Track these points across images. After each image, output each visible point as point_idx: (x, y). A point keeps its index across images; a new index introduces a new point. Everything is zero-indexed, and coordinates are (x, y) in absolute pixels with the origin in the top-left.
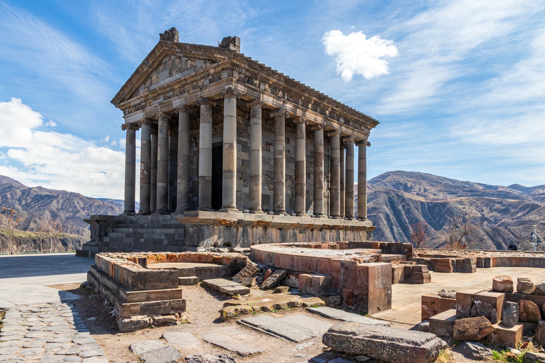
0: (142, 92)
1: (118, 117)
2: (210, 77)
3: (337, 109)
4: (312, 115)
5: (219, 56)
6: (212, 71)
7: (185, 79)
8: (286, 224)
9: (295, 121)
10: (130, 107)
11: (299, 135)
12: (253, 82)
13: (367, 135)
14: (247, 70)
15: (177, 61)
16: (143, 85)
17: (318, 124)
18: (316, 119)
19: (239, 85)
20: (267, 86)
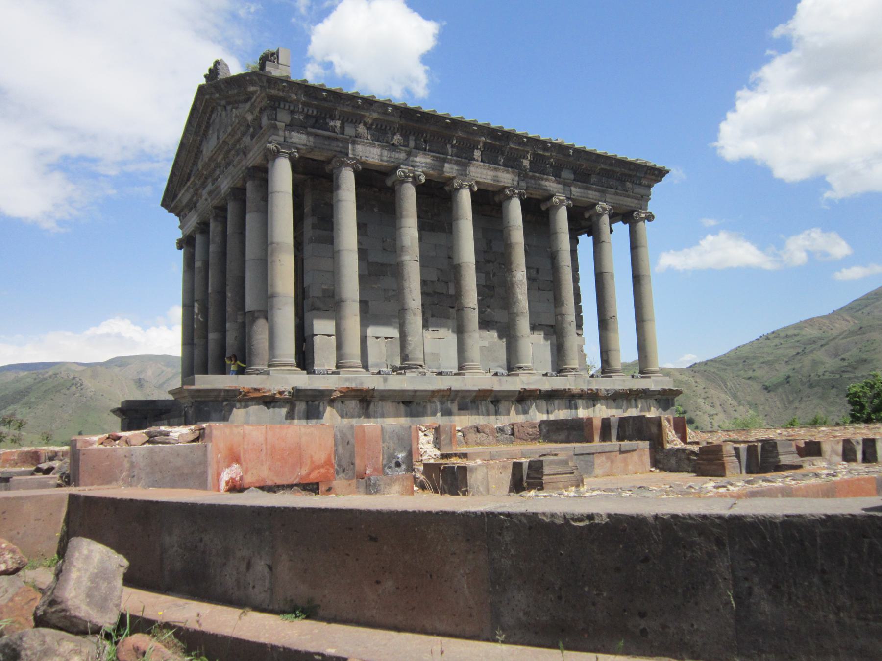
2: (252, 130)
3: (548, 154)
4: (485, 172)
6: (250, 118)
8: (416, 391)
9: (447, 188)
12: (327, 124)
13: (646, 198)
14: (304, 104)
15: (224, 113)
17: (505, 187)
19: (294, 134)
20: (361, 129)
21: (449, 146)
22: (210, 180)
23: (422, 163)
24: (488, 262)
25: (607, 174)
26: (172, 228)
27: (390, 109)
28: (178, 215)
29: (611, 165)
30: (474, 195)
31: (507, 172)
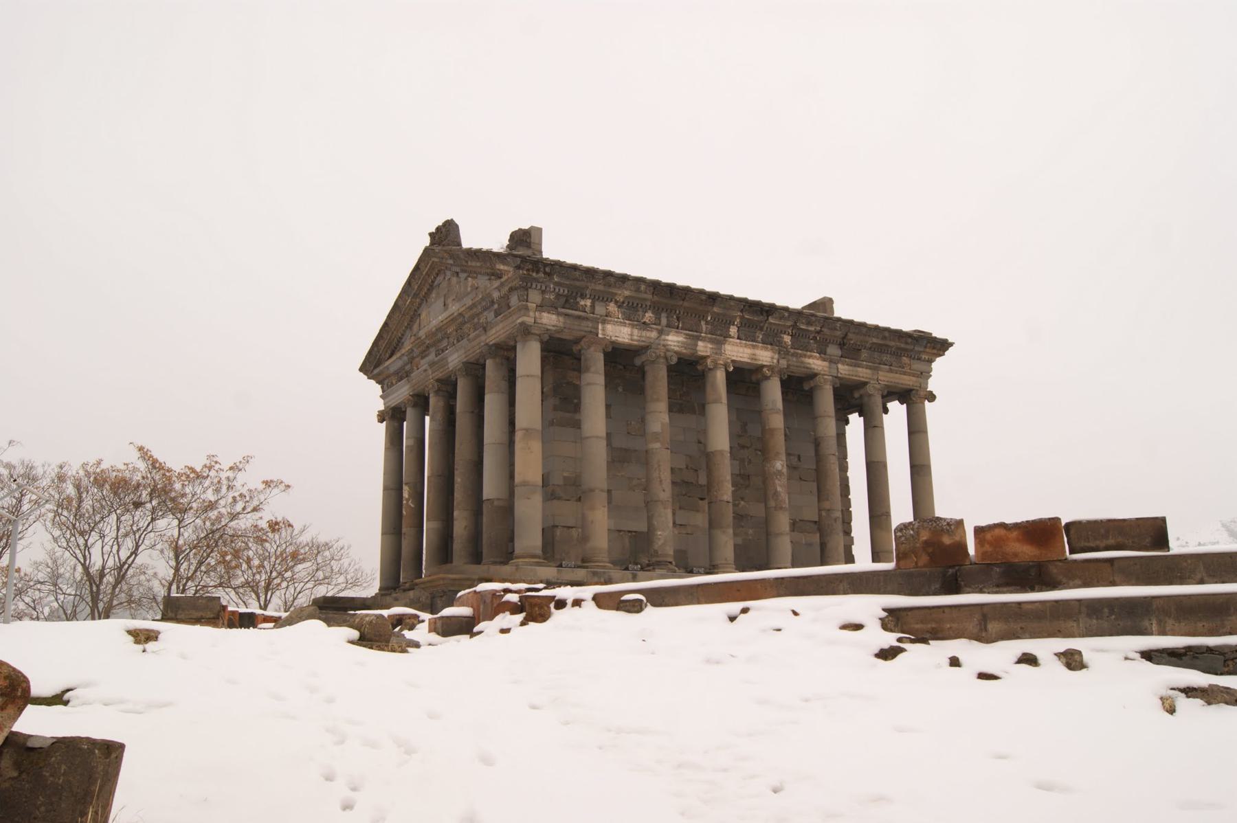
0: (407, 346)
1: (371, 396)
2: (496, 306)
3: (812, 329)
4: (741, 350)
5: (502, 267)
6: (496, 295)
7: (460, 314)
9: (699, 368)
10: (388, 377)
11: (710, 396)
13: (926, 374)
15: (454, 279)
16: (408, 333)
17: (763, 366)
18: (753, 357)
19: (545, 314)
20: (612, 307)
21: (703, 323)
22: (433, 350)
23: (675, 340)
24: (743, 447)
25: (881, 349)
26: (370, 397)
27: (643, 287)
28: (378, 382)
29: (884, 338)
30: (727, 373)
31: (766, 349)
